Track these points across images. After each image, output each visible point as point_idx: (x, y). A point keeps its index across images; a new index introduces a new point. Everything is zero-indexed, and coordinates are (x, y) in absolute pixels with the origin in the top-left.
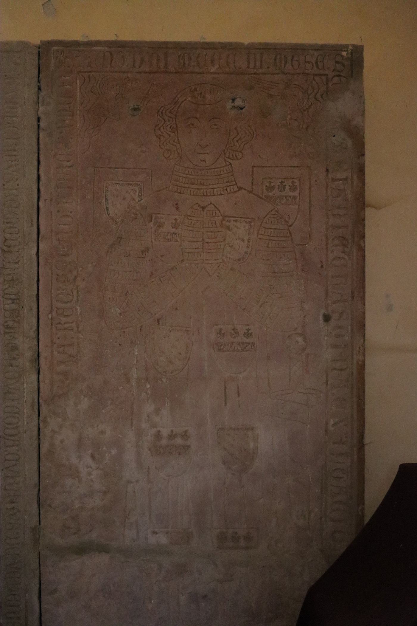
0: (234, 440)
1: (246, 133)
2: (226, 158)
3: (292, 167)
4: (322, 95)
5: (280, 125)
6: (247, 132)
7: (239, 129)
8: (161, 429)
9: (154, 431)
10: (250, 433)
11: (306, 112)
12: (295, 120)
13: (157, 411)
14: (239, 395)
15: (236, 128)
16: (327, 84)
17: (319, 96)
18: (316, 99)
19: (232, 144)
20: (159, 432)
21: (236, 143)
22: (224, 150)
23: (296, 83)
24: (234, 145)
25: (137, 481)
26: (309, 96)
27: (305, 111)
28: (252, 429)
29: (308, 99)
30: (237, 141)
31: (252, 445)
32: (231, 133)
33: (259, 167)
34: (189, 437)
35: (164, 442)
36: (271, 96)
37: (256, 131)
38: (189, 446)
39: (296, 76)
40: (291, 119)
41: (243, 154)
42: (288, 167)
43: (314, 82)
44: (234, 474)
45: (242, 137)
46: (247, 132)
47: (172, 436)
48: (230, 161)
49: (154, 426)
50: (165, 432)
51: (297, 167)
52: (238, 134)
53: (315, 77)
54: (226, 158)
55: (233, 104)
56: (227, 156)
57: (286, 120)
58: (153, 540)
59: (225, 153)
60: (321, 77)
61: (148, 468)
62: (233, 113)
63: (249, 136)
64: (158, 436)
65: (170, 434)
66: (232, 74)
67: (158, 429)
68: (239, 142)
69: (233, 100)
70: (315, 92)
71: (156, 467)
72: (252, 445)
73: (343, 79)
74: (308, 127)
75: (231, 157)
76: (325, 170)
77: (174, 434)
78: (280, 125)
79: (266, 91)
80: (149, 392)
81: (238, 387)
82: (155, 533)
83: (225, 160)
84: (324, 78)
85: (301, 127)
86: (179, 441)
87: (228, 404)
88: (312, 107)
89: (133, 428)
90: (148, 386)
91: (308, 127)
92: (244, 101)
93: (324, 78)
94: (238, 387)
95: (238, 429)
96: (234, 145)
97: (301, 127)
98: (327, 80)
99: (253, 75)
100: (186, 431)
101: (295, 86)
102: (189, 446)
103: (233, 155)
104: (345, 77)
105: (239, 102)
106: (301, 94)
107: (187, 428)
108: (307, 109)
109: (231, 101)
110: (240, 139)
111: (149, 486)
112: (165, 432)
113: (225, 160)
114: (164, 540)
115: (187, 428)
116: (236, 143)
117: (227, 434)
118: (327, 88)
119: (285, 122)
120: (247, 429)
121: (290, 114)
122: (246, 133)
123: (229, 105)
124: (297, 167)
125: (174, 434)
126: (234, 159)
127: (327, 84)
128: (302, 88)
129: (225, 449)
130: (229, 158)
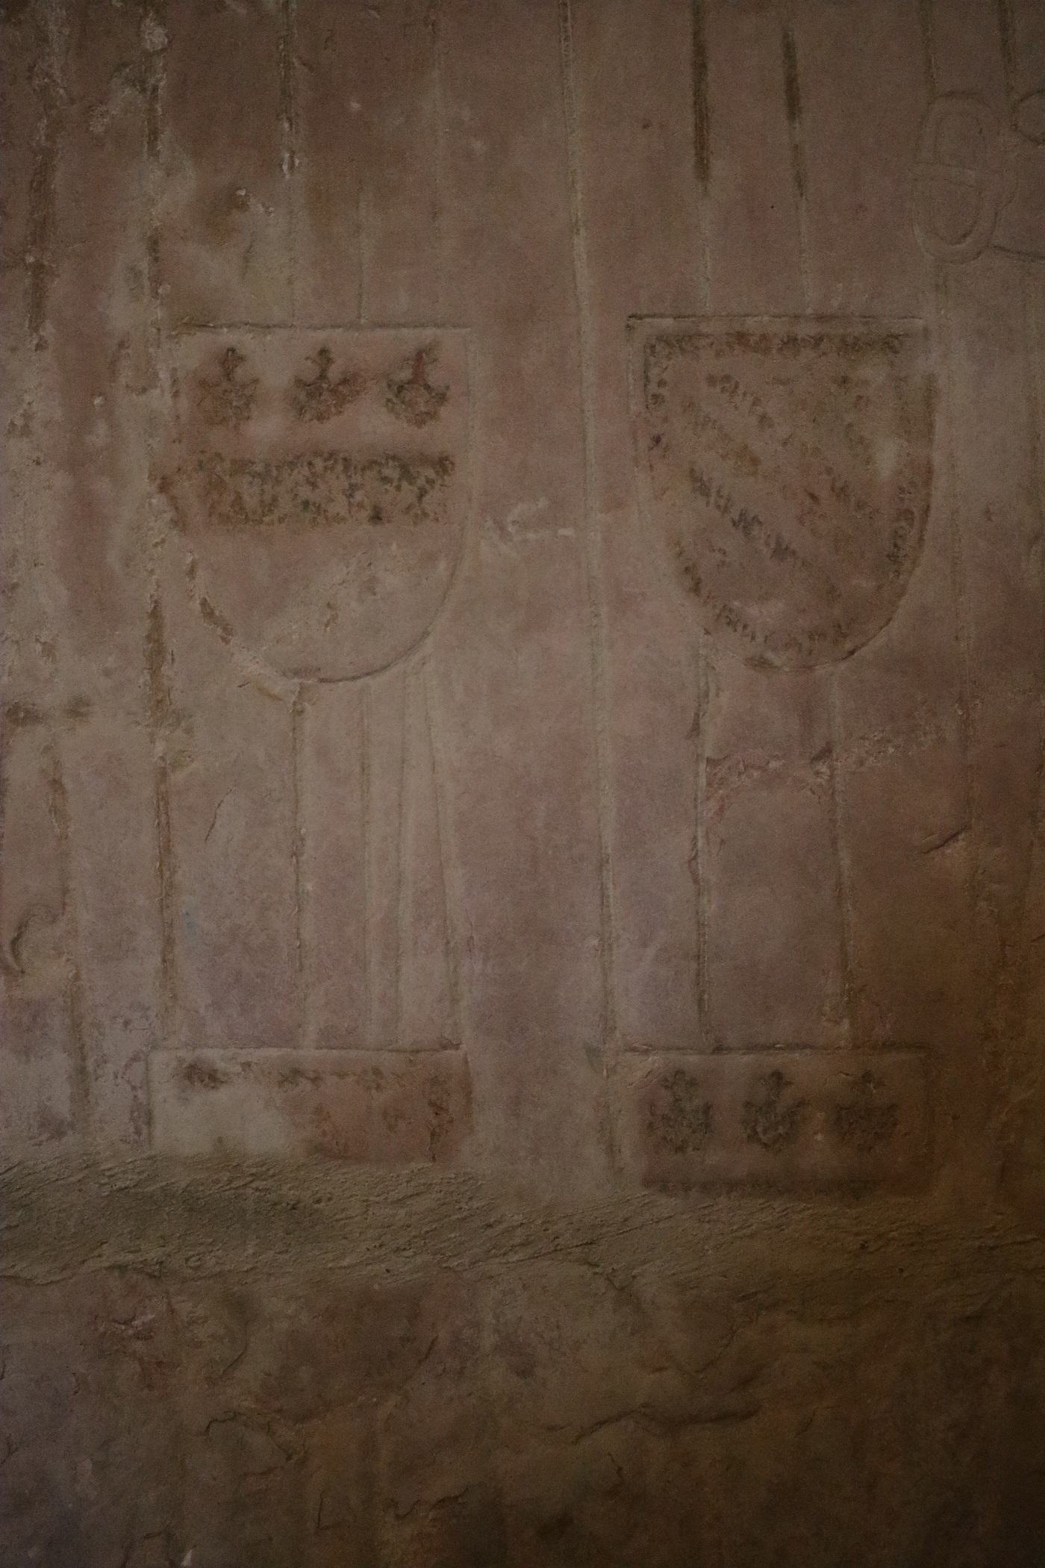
0: (763, 419)
8: (245, 341)
9: (192, 352)
10: (873, 372)
13: (219, 213)
14: (793, 109)
20: (230, 359)
25: (77, 709)
28: (890, 344)
31: (888, 456)
34: (442, 398)
35: (267, 429)
38: (443, 464)
44: (760, 664)
47: (322, 388)
49: (196, 318)
50: (275, 363)
58: (184, 1127)
61: (155, 614)
64: (225, 387)
65: (310, 372)
67: (228, 338)
71: (208, 612)
72: (888, 456)
77: (334, 373)
80: (162, 81)
81: (789, 48)
82: (199, 1075)
86: (372, 423)
87: (718, 167)
89: (49, 330)
90: (155, 36)
94: (789, 48)
95: (791, 342)
100: (421, 358)
102: (443, 464)
107: (429, 334)
111: (160, 748)
112: (275, 363)
114: (264, 1128)
115: (429, 334)
117: (711, 380)
120: (851, 347)
125: (334, 373)
129: (700, 485)
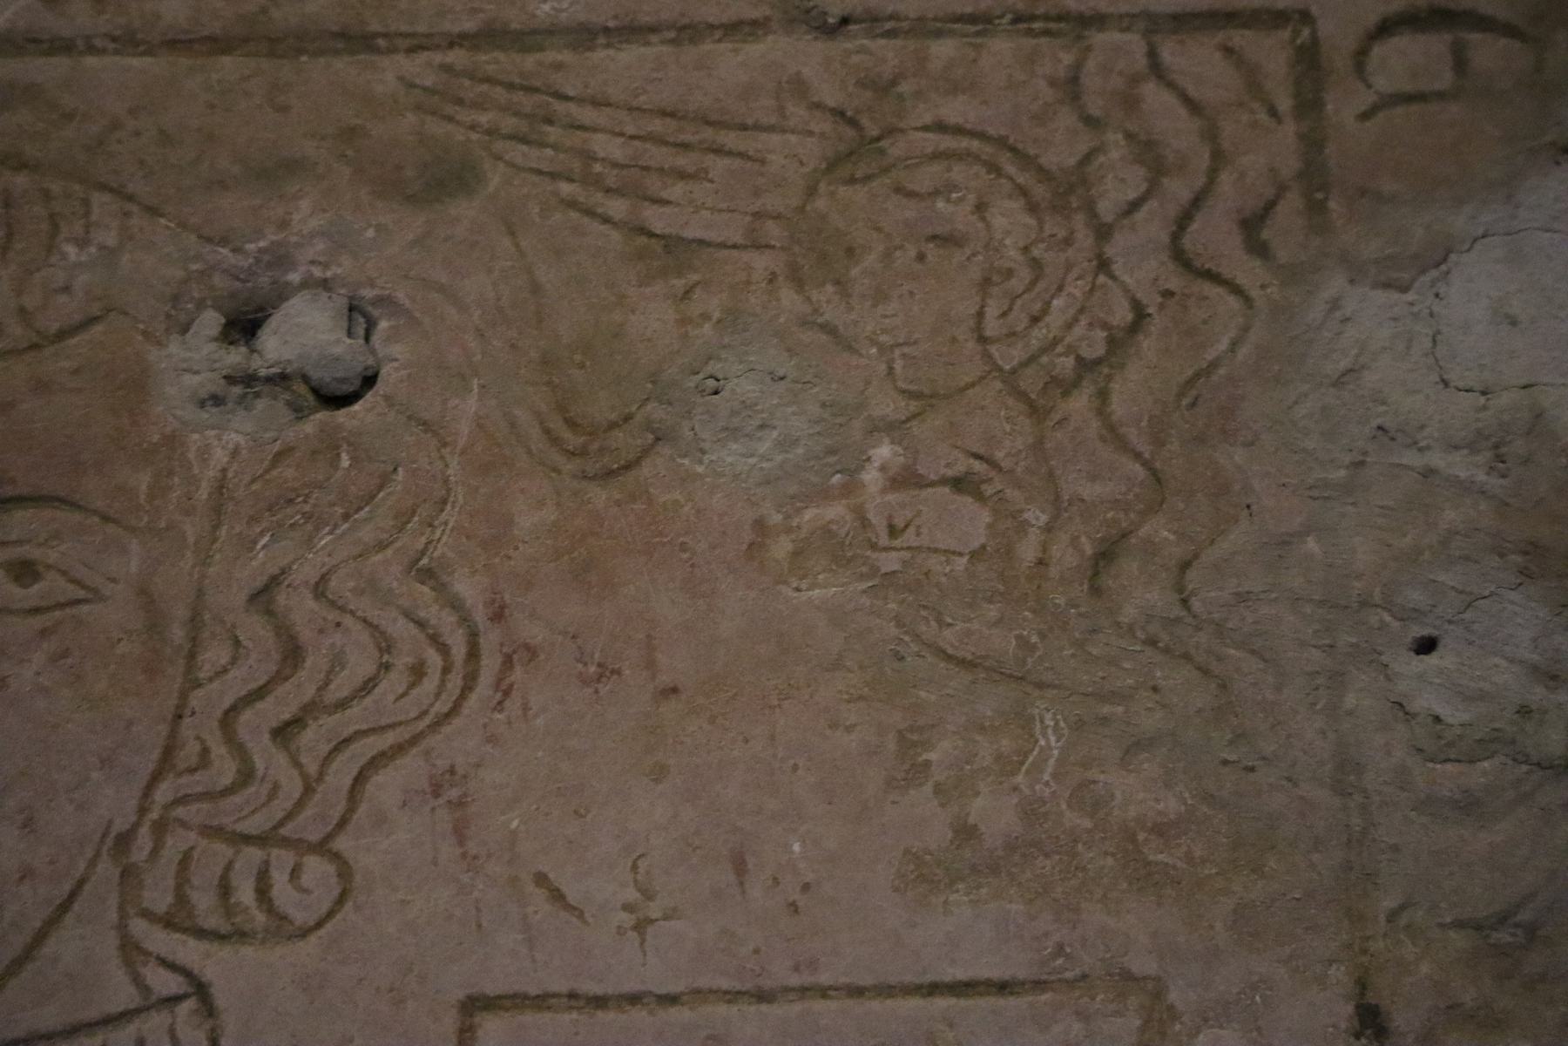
1: (386, 645)
2: (138, 926)
3: (934, 989)
4: (1252, 226)
5: (781, 548)
6: (400, 628)
7: (300, 607)
11: (1080, 403)
12: (959, 484)
15: (262, 597)
16: (1309, 105)
17: (1216, 236)
18: (1181, 258)
19: (225, 770)
21: (267, 758)
22: (124, 841)
23: (955, 110)
24: (246, 775)
26: (1103, 232)
27: (1067, 387)
29: (1103, 265)
30: (284, 733)
32: (214, 654)
33: (541, 1001)
36: (675, 252)
37: (498, 615)
39: (943, 50)
40: (905, 479)
41: (345, 871)
42: (887, 991)
43: (1152, 92)
45: (341, 687)
46: (400, 628)
48: (189, 951)
51: (1003, 987)
52: (293, 654)
53: (1169, 53)
54: (138, 926)
55: (235, 357)
56: (159, 898)
57: (851, 488)
59: (129, 876)
60: (1240, 38)
62: (229, 441)
63: (418, 672)
66: (219, 45)
68: (313, 739)
69: (244, 326)
70: (1179, 190)
73: (1487, 52)
74: (1105, 556)
75: (204, 902)
76: (1346, 1010)
78: (781, 548)
79: (617, 207)
83: (131, 950)
84: (1272, 52)
85: (1028, 551)
88: (1148, 344)
91: (1105, 556)
92: (359, 317)
93: (1272, 52)
96: (246, 775)
97: (1028, 551)
98: (1309, 58)
99: (457, 57)
101: (933, 141)
103: (225, 889)
104: (1510, 31)
105: (305, 332)
106: (1009, 219)
108: (1085, 366)
109: (211, 321)
110: (311, 710)
113: (131, 950)
116: (267, 758)
118: (1312, 143)
119: (835, 511)
121: (892, 429)
122: (386, 645)
123: (196, 356)
124: (1003, 987)
126: (241, 935)
127: (1309, 105)
128: (1026, 161)
130: (177, 920)
